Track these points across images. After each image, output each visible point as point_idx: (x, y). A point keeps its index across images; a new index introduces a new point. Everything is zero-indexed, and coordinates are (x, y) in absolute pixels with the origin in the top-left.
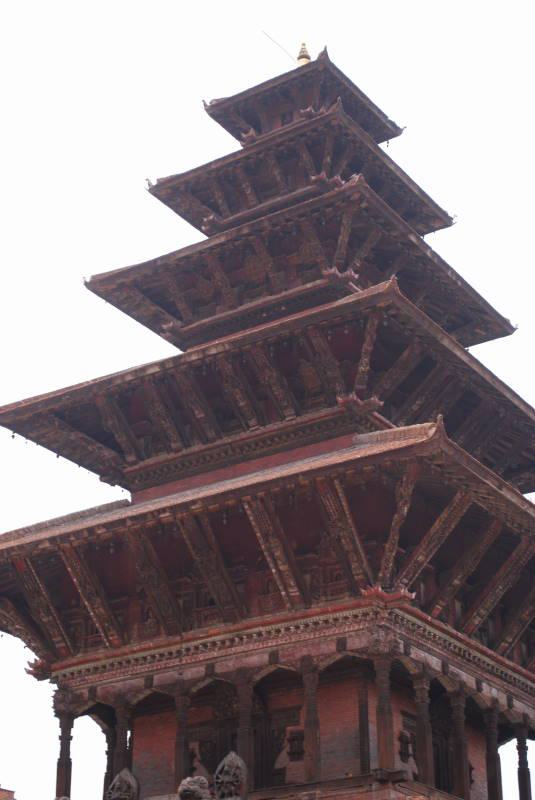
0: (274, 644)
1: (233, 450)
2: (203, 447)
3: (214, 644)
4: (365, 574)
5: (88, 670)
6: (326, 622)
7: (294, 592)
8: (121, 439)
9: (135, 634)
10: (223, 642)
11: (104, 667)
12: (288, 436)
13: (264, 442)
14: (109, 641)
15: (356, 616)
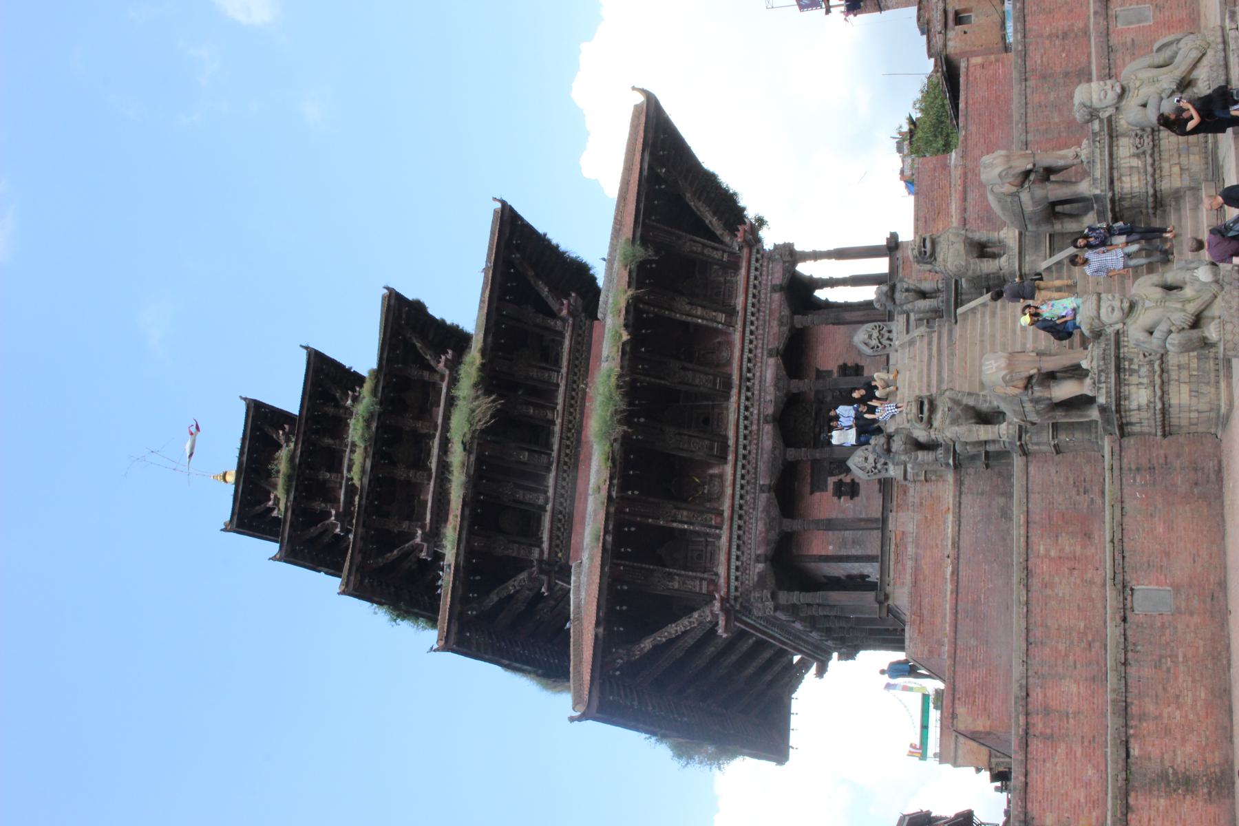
0: (759, 351)
1: (568, 439)
2: (554, 467)
3: (747, 408)
4: (724, 251)
5: (738, 558)
6: (754, 296)
7: (722, 317)
8: (514, 551)
9: (716, 505)
10: (747, 399)
11: (739, 537)
12: (574, 382)
13: (572, 406)
14: (716, 528)
15: (756, 269)
